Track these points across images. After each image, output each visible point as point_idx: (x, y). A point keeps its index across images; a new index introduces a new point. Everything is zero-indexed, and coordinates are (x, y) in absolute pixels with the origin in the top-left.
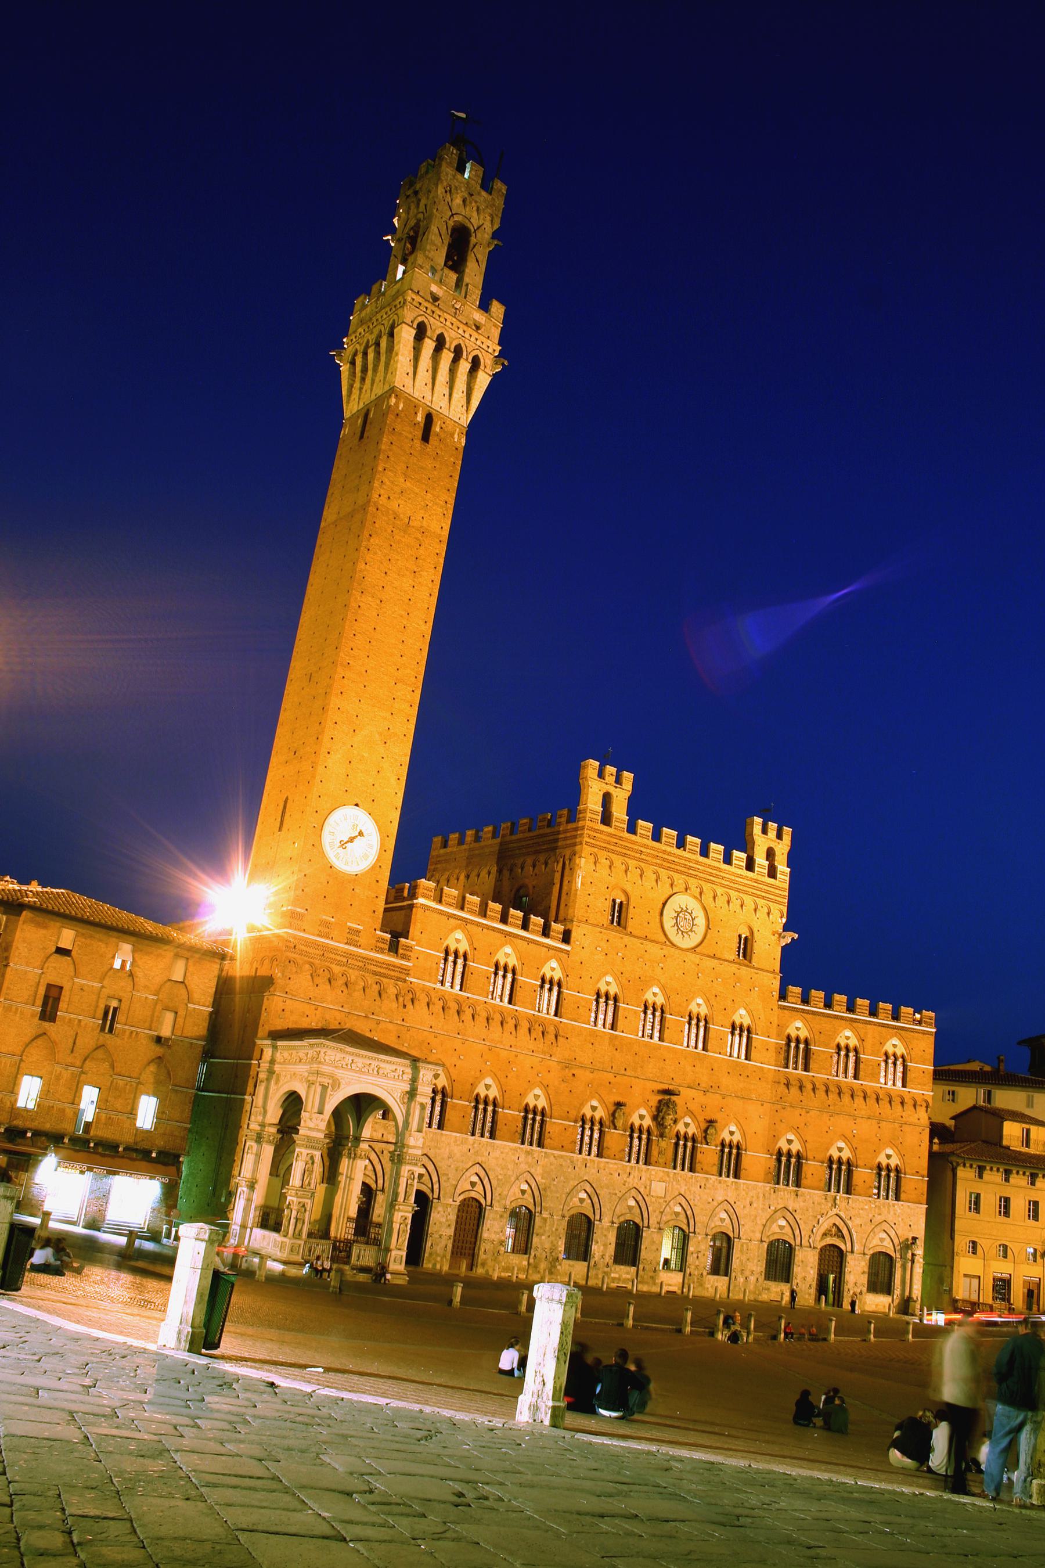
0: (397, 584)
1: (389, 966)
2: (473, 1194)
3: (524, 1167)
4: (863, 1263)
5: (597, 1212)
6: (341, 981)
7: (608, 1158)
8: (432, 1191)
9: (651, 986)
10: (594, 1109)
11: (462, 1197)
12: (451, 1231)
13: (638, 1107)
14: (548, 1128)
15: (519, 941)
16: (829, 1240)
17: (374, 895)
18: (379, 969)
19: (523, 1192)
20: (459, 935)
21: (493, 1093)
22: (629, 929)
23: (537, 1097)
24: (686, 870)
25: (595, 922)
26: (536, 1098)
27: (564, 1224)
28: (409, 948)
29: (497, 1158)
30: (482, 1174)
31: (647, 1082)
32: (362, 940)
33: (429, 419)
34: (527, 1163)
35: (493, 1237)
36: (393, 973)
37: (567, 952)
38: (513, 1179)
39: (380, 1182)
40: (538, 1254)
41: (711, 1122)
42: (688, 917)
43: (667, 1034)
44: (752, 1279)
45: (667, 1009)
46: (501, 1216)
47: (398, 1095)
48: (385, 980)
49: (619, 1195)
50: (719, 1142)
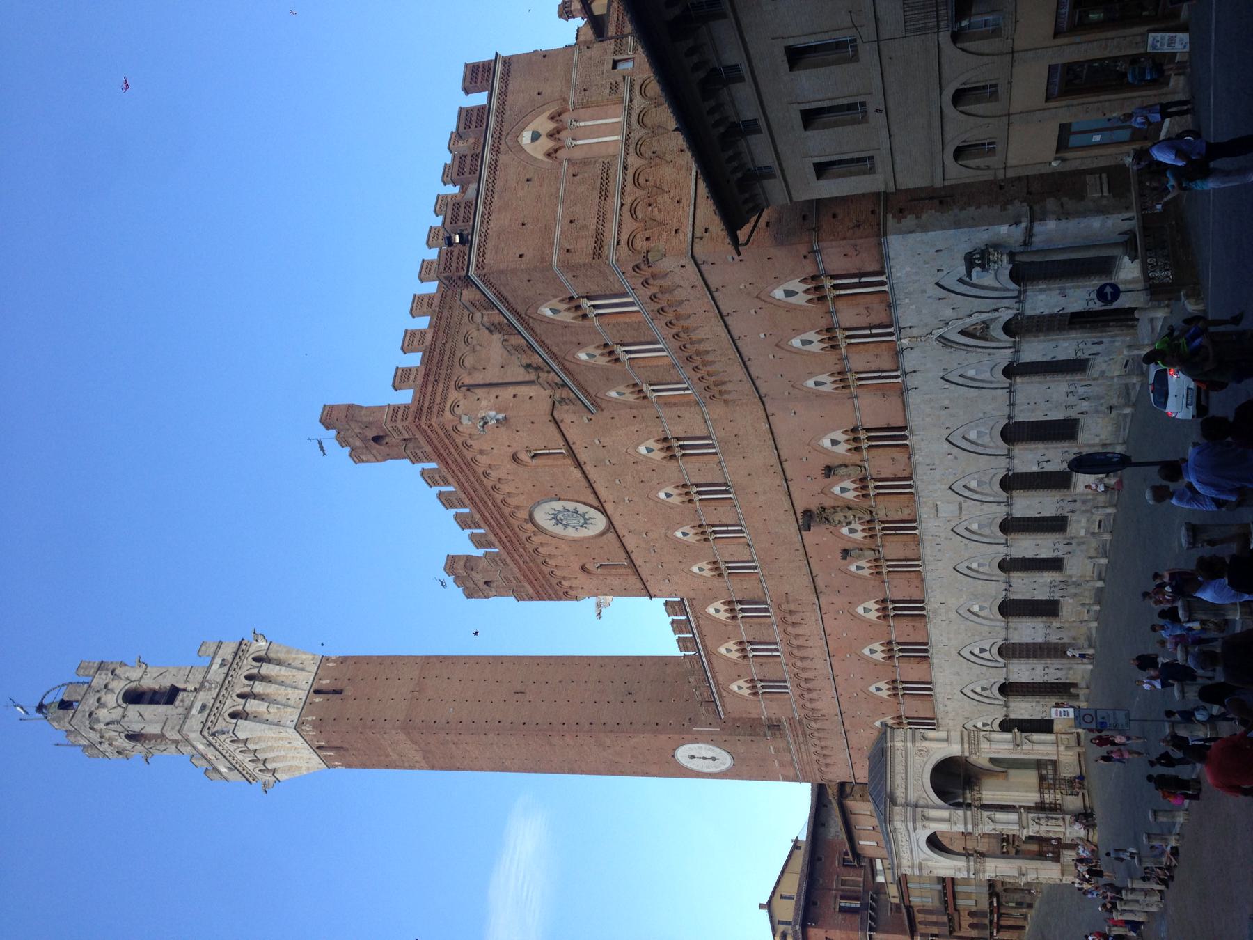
2: (995, 650)
3: (953, 615)
4: (1042, 297)
11: (1000, 659)
13: (841, 536)
15: (709, 644)
16: (997, 331)
19: (981, 608)
21: (877, 646)
26: (869, 610)
28: (769, 719)
33: (319, 748)
37: (690, 600)
41: (829, 471)
42: (560, 516)
44: (1081, 391)
48: (808, 731)
49: (967, 541)
50: (855, 458)
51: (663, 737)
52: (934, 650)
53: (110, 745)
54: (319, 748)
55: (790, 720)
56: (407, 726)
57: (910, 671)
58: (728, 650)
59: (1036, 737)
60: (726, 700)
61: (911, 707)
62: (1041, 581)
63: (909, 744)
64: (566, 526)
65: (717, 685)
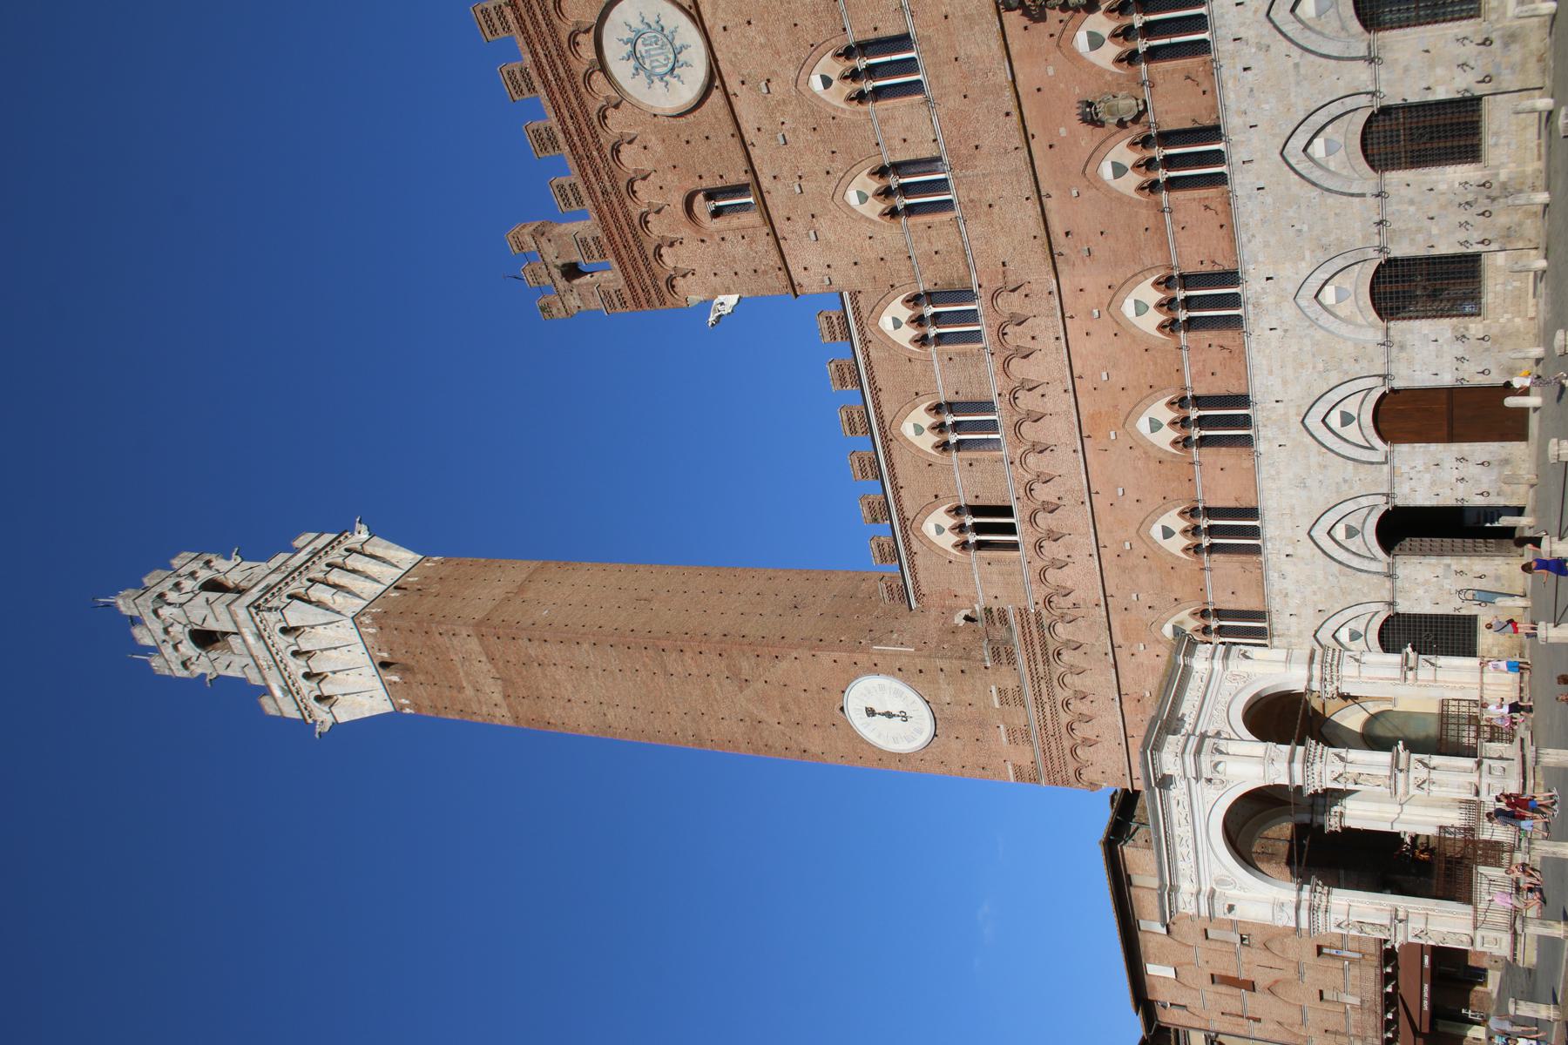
0: (569, 687)
1: (1029, 643)
3: (1289, 311)
5: (1350, 103)
6: (1077, 705)
7: (1214, 108)
8: (1373, 507)
9: (814, 95)
10: (1119, 170)
11: (1377, 442)
12: (1446, 452)
13: (1076, 57)
14: (1191, 267)
17: (942, 675)
18: (1039, 657)
20: (929, 528)
22: (745, 179)
23: (1140, 308)
24: (568, 87)
25: (774, 254)
26: (1141, 306)
27: (1396, 178)
28: (988, 611)
29: (1285, 383)
30: (1321, 409)
31: (1014, 49)
32: (1010, 684)
33: (384, 665)
34: (1278, 304)
35: (1448, 360)
36: (1035, 634)
37: (854, 295)
38: (1319, 335)
39: (1374, 607)
40: (1475, 236)
42: (639, 46)
43: (890, 30)
45: (840, 43)
46: (1402, 347)
47: (1211, 793)
49: (1296, 53)
51: (825, 658)
52: (1257, 413)
53: (175, 647)
54: (384, 665)
55: (1023, 613)
56: (482, 628)
57: (1216, 476)
58: (915, 428)
59: (1443, 661)
60: (919, 560)
61: (1225, 582)
62: (1443, 187)
63: (1218, 664)
64: (650, 76)
65: (903, 521)
